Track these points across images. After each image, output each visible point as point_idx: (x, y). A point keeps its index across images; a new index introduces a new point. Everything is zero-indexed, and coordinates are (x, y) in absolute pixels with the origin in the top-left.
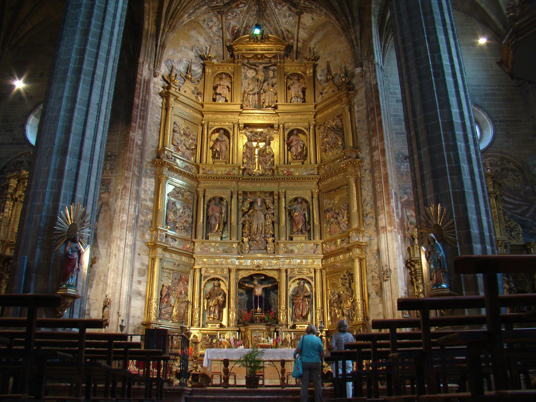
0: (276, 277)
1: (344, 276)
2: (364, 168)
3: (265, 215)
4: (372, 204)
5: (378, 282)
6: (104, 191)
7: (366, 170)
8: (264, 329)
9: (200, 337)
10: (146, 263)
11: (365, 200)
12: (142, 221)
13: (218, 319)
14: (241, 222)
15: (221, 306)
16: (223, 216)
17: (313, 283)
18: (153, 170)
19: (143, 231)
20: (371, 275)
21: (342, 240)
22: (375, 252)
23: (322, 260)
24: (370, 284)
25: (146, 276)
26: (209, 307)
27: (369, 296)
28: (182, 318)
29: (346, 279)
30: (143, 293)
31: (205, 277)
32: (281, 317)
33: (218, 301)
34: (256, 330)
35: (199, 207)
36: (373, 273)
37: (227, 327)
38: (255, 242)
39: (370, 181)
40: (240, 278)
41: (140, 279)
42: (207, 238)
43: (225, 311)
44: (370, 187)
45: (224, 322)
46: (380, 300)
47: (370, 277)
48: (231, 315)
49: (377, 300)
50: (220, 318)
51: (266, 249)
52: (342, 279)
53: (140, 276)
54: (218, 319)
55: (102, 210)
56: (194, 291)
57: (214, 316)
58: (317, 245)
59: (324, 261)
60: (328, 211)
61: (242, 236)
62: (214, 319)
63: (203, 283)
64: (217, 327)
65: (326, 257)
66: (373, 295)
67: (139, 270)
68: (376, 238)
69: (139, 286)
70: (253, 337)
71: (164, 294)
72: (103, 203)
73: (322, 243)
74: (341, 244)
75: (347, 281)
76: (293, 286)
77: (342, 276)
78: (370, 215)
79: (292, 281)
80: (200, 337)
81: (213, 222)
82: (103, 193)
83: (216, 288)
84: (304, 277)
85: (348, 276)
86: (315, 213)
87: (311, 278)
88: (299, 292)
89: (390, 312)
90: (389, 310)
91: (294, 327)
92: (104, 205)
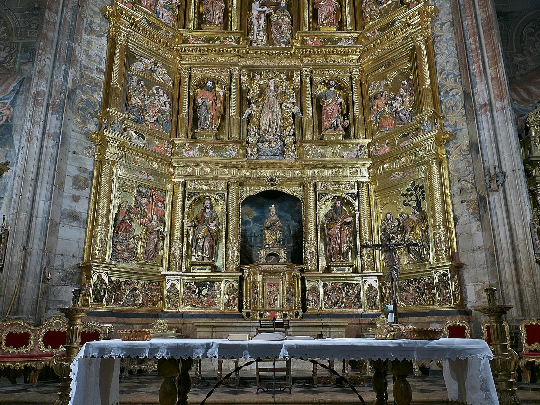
0: (299, 196)
1: (408, 190)
2: (440, 22)
3: (281, 105)
4: (457, 73)
5: (473, 196)
6: (26, 61)
7: (443, 24)
8: (284, 272)
9: (180, 286)
10: (90, 168)
11: (443, 70)
12: (82, 101)
13: (209, 259)
14: (245, 115)
15: (214, 238)
16: (218, 105)
17: (356, 204)
18: (103, 26)
19: (84, 116)
20: (459, 186)
21: (404, 136)
22: (465, 148)
23: (369, 169)
24: (457, 200)
25: (88, 190)
26: (195, 239)
27: (456, 220)
28: (151, 256)
29: (411, 195)
30: (84, 216)
31: (191, 195)
32: (309, 255)
33: (209, 231)
34: (270, 274)
35: (181, 90)
36: (463, 182)
37: (223, 270)
38: (267, 144)
39: (452, 39)
40: (245, 196)
41: (77, 193)
42: (194, 136)
43: (222, 245)
44: (452, 48)
45: (220, 262)
46: (478, 226)
47: (456, 188)
48: (230, 252)
49: (475, 226)
50: (213, 257)
51: (283, 153)
52: (403, 195)
53: (78, 189)
54: (209, 259)
55: (22, 89)
56: (173, 215)
57: (203, 254)
58: (362, 146)
59: (371, 170)
60: (376, 97)
61: (247, 136)
62: (203, 258)
63: (188, 203)
64: (208, 270)
65: (377, 161)
66: (465, 217)
67: (76, 179)
68: (466, 126)
69: (74, 204)
70: (266, 287)
71: (120, 218)
72: (24, 78)
73: (369, 144)
74: (400, 142)
75: (414, 198)
76: (325, 208)
77: (404, 192)
78: (454, 91)
79: (323, 200)
80: (180, 286)
81: (202, 112)
82: (24, 63)
83: (208, 211)
84: (342, 194)
85: (415, 190)
86: (355, 100)
87: (353, 196)
88: (335, 216)
89: (504, 245)
90: (504, 241)
91: (328, 269)
92: (25, 83)
